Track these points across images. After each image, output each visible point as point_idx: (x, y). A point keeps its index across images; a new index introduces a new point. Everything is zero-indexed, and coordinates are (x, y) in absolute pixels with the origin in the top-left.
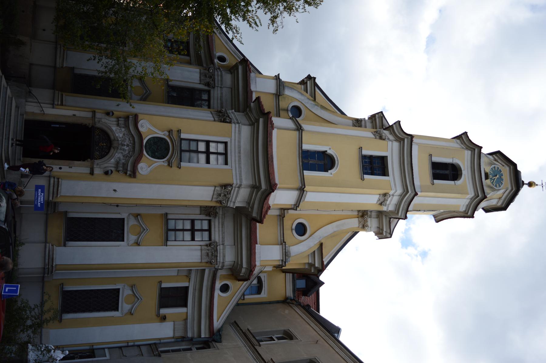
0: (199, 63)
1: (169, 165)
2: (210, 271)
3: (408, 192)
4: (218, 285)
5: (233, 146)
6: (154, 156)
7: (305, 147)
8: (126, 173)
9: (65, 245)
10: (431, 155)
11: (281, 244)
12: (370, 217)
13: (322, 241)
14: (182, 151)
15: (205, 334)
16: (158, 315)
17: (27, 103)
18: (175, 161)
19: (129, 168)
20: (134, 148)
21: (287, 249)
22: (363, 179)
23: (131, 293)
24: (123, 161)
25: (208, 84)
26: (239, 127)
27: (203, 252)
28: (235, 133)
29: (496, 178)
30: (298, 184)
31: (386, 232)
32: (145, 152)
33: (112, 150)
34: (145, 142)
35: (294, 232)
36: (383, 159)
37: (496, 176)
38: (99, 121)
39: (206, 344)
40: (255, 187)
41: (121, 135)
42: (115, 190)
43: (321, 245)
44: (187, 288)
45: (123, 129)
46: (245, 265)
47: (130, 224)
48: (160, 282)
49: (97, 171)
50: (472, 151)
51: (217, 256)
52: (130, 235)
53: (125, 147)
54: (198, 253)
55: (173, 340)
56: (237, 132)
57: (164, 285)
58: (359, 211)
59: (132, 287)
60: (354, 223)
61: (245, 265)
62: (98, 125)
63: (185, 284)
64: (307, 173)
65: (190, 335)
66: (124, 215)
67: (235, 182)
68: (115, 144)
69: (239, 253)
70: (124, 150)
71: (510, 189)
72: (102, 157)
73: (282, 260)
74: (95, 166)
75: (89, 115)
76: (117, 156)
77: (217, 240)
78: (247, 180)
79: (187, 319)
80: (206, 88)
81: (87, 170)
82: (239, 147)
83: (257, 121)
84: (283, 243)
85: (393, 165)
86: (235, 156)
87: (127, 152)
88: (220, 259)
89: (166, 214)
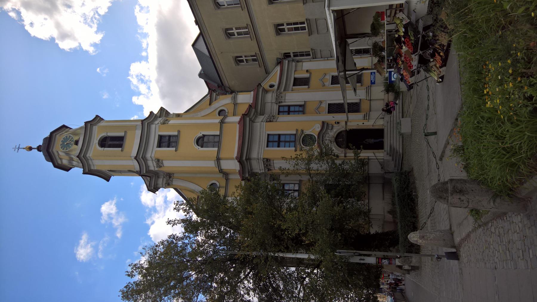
1: (303, 131)
2: (281, 90)
6: (311, 135)
8: (327, 123)
9: (360, 100)
11: (236, 104)
15: (285, 62)
16: (310, 74)
17: (383, 158)
18: (299, 132)
19: (326, 125)
20: (323, 138)
21: (233, 101)
22: (179, 132)
23: (325, 83)
24: (329, 130)
26: (258, 156)
27: (284, 99)
28: (261, 153)
29: (67, 142)
32: (316, 137)
33: (335, 136)
38: (342, 151)
39: (287, 56)
40: (252, 121)
43: (210, 104)
44: (294, 85)
49: (344, 124)
50: (86, 156)
51: (276, 96)
52: (325, 107)
53: (328, 139)
54: (286, 98)
55: (303, 61)
56: (260, 153)
57: (307, 87)
59: (324, 85)
62: (343, 150)
63: (294, 87)
64: (218, 133)
65: (294, 63)
68: (333, 140)
69: (263, 98)
70: (328, 137)
71: (57, 136)
74: (345, 126)
75: (348, 155)
76: (332, 134)
79: (295, 71)
82: (259, 145)
83: (246, 159)
86: (262, 139)
87: (326, 136)
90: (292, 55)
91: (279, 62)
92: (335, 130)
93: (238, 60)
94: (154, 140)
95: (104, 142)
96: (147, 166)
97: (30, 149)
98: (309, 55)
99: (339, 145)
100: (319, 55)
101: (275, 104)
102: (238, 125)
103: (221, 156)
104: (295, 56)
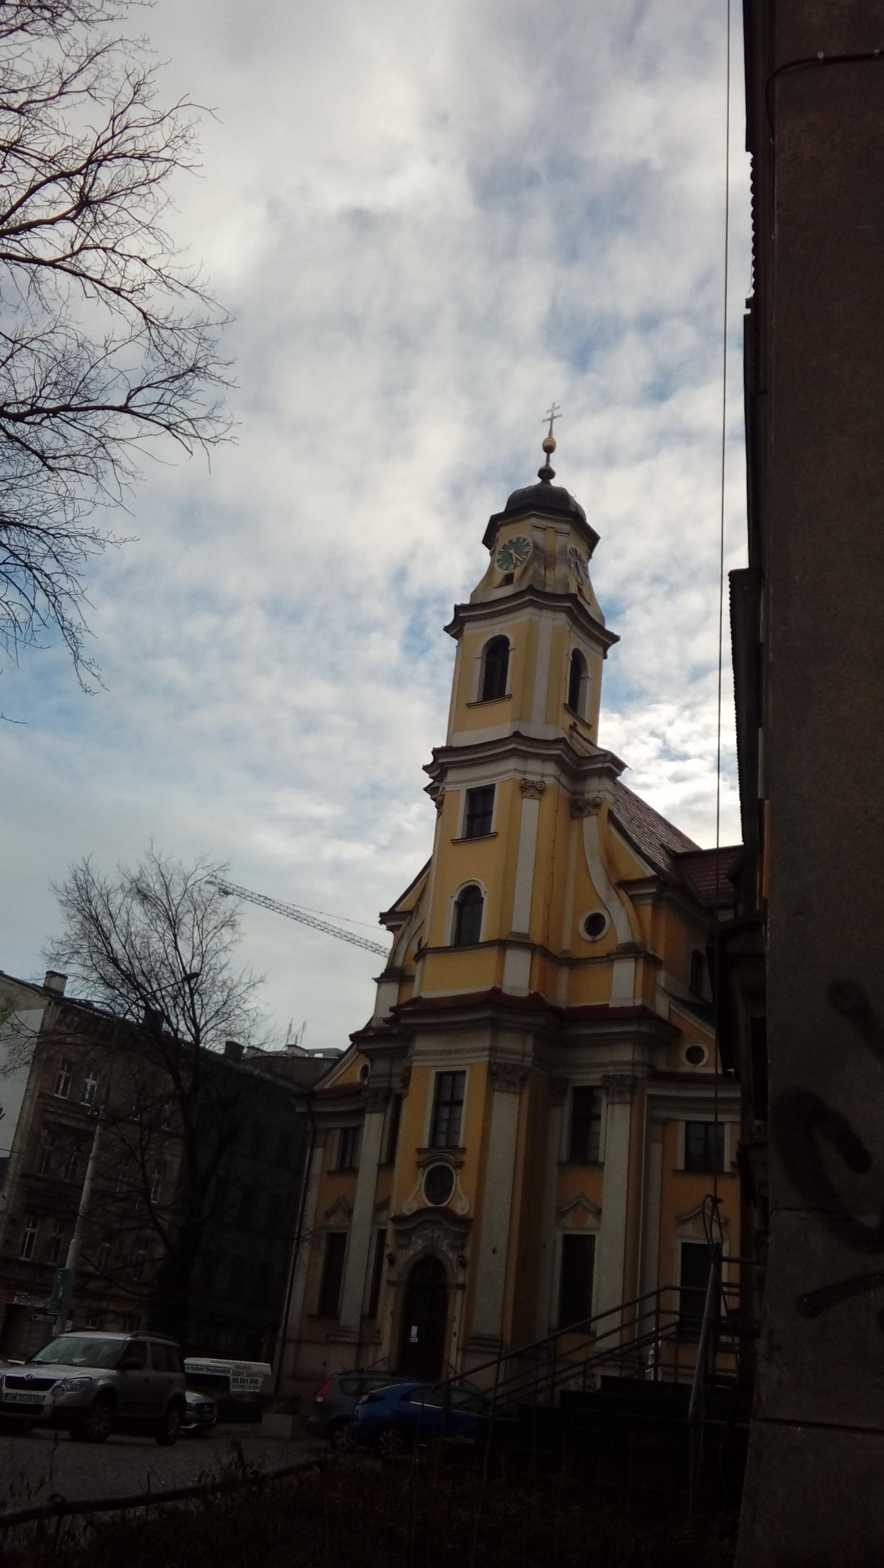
0: (360, 1114)
3: (514, 749)
4: (687, 1067)
5: (444, 1063)
7: (447, 941)
10: (469, 705)
11: (612, 961)
12: (582, 793)
13: (615, 881)
14: (447, 1147)
25: (386, 1099)
29: (515, 555)
31: (604, 762)
32: (444, 1205)
34: (431, 1205)
35: (598, 937)
36: (473, 794)
37: (511, 555)
40: (495, 1026)
41: (420, 1242)
42: (494, 1251)
44: (689, 1124)
45: (413, 1239)
46: (633, 1028)
47: (572, 1226)
48: (676, 1172)
49: (461, 1279)
58: (573, 817)
59: (681, 1221)
60: (591, 825)
61: (633, 1028)
63: (682, 1126)
66: (559, 1234)
67: (487, 1059)
73: (636, 958)
77: (598, 1076)
78: (485, 1041)
80: (391, 1101)
81: (459, 1293)
82: (442, 1052)
84: (610, 958)
88: (627, 1071)
89: (560, 1164)
101: (602, 1075)
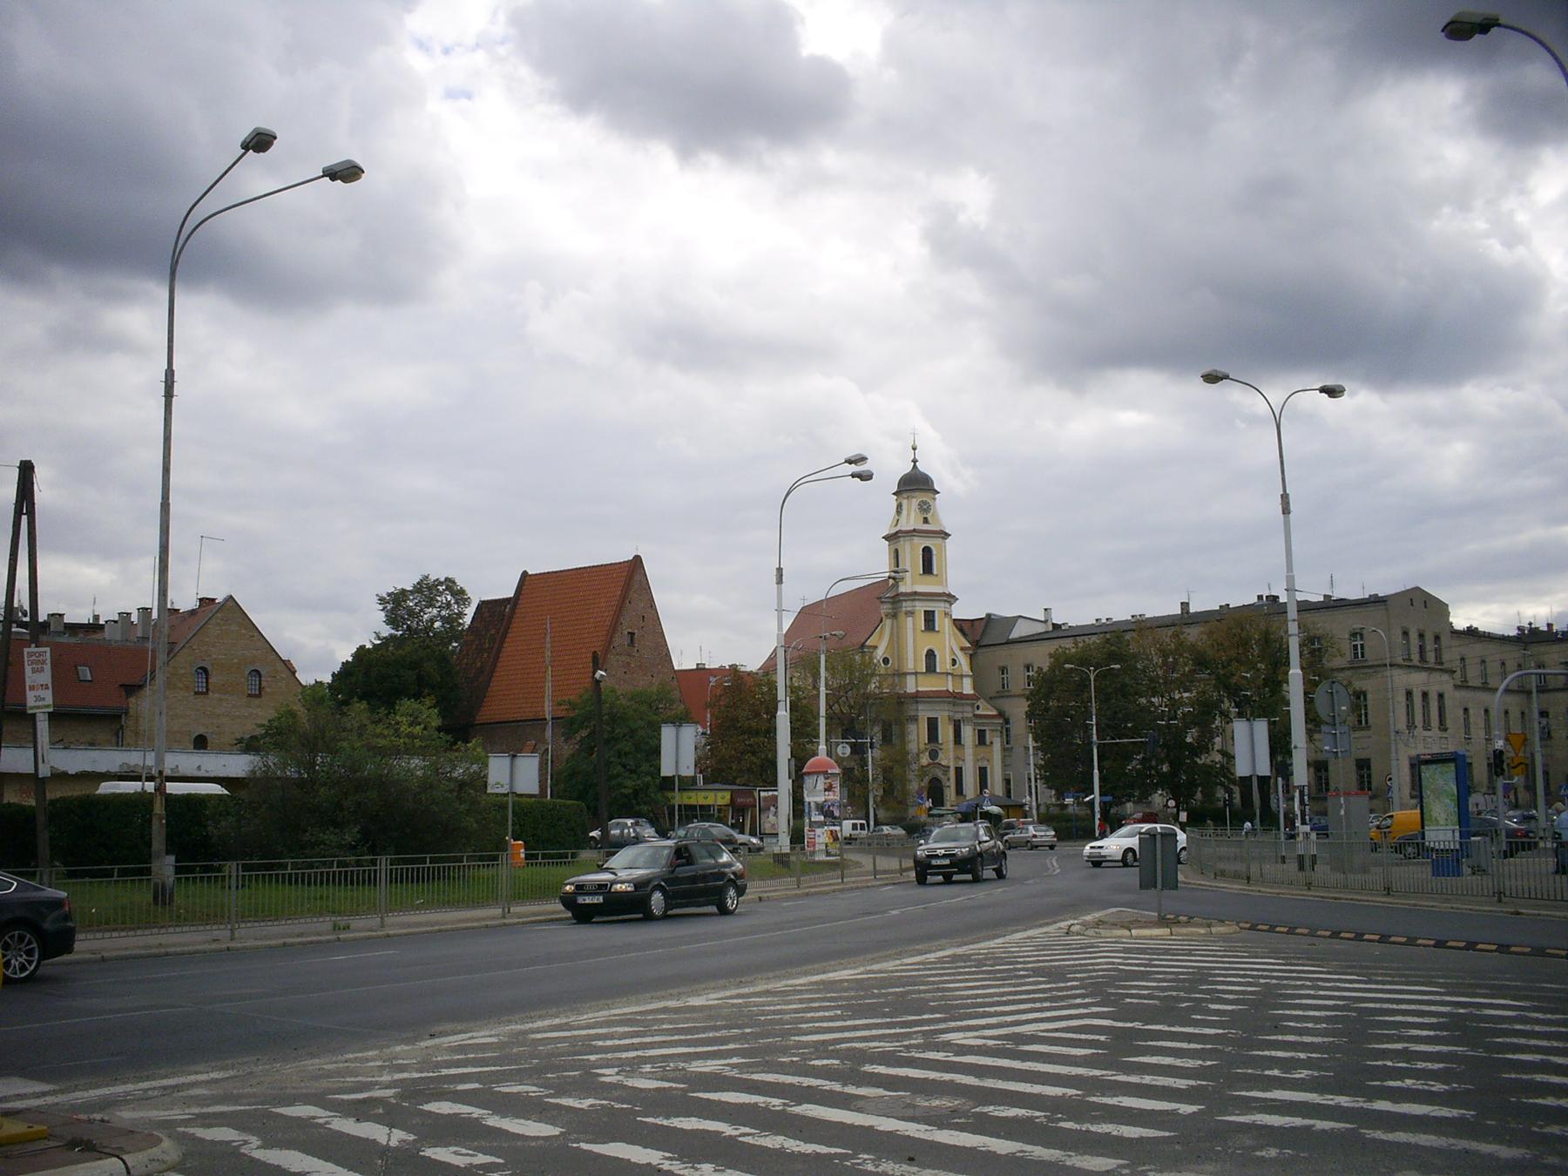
7: (924, 671)
30: (945, 675)
39: (1007, 721)
49: (948, 784)
64: (938, 670)
65: (999, 728)
72: (941, 782)
76: (940, 774)
85: (930, 606)
90: (1008, 726)
91: (1001, 714)
92: (942, 776)
93: (1003, 670)
94: (930, 606)
95: (927, 552)
96: (905, 601)
97: (914, 449)
98: (1007, 743)
99: (931, 781)
100: (1007, 754)
102: (945, 689)
103: (919, 676)
104: (1007, 729)
